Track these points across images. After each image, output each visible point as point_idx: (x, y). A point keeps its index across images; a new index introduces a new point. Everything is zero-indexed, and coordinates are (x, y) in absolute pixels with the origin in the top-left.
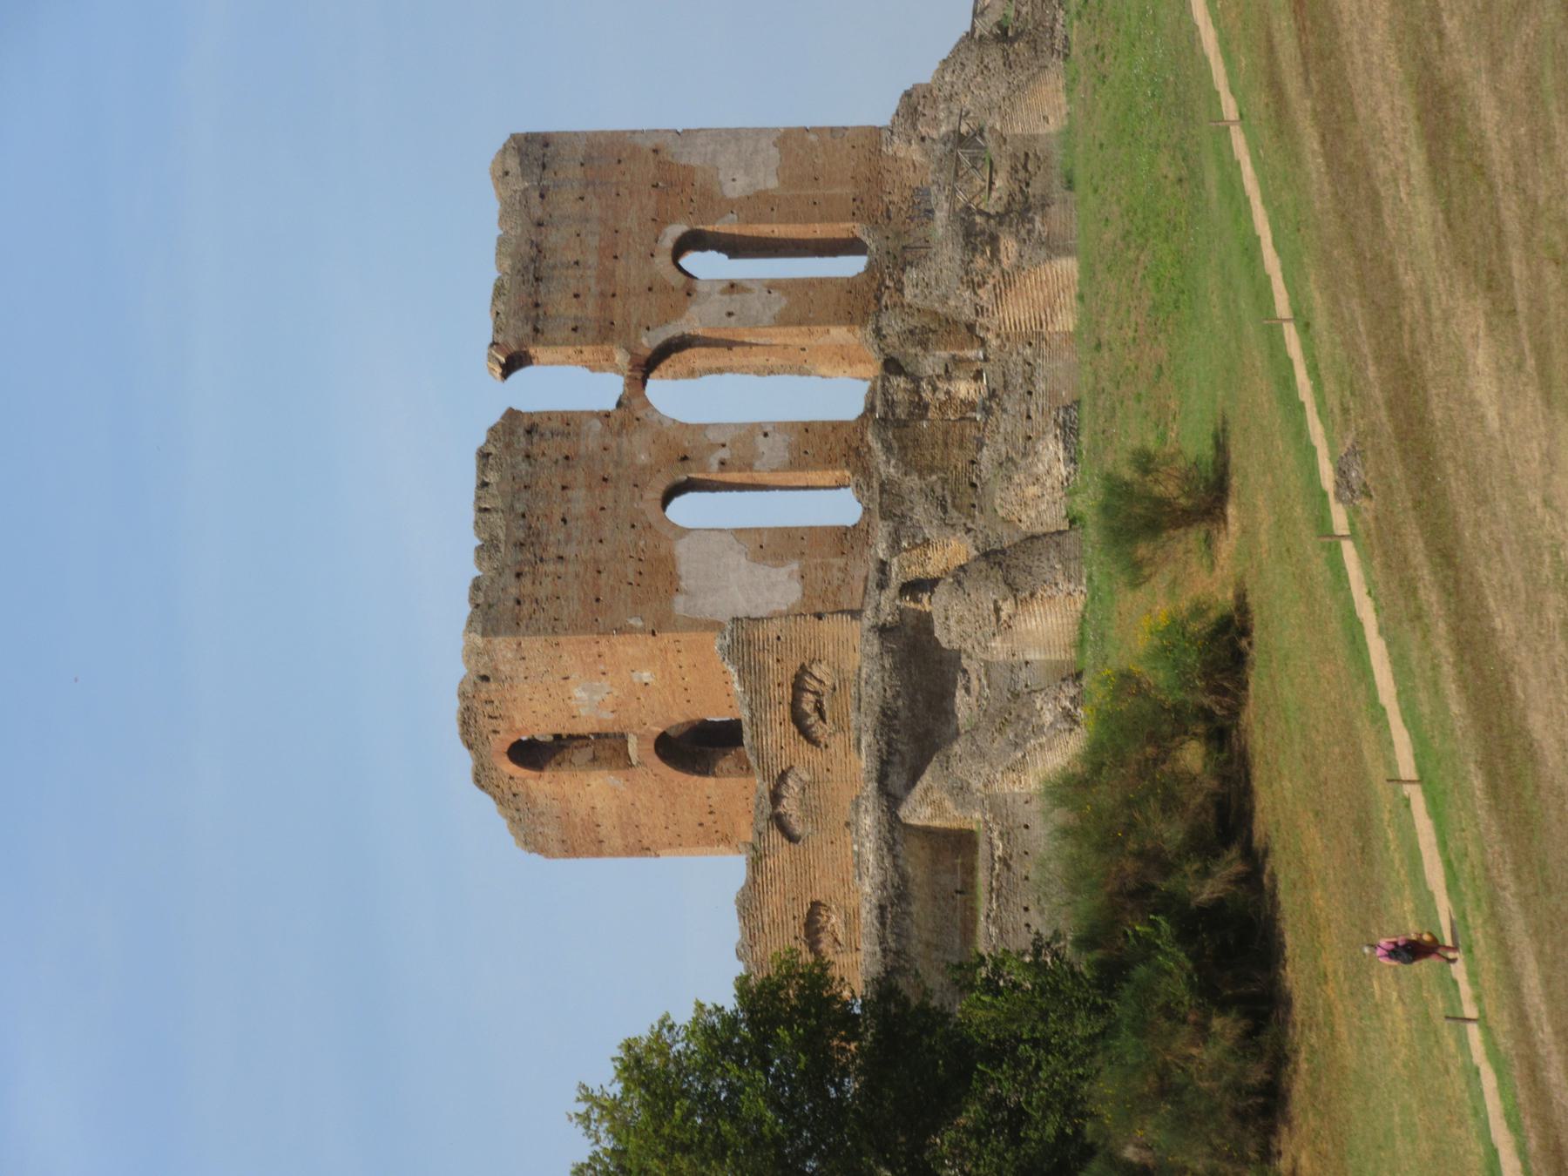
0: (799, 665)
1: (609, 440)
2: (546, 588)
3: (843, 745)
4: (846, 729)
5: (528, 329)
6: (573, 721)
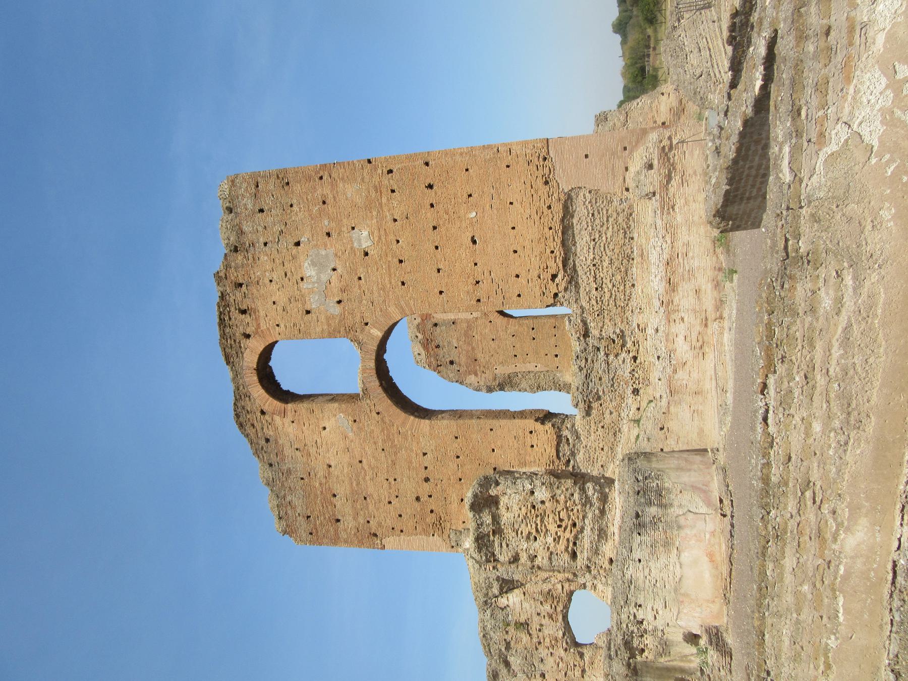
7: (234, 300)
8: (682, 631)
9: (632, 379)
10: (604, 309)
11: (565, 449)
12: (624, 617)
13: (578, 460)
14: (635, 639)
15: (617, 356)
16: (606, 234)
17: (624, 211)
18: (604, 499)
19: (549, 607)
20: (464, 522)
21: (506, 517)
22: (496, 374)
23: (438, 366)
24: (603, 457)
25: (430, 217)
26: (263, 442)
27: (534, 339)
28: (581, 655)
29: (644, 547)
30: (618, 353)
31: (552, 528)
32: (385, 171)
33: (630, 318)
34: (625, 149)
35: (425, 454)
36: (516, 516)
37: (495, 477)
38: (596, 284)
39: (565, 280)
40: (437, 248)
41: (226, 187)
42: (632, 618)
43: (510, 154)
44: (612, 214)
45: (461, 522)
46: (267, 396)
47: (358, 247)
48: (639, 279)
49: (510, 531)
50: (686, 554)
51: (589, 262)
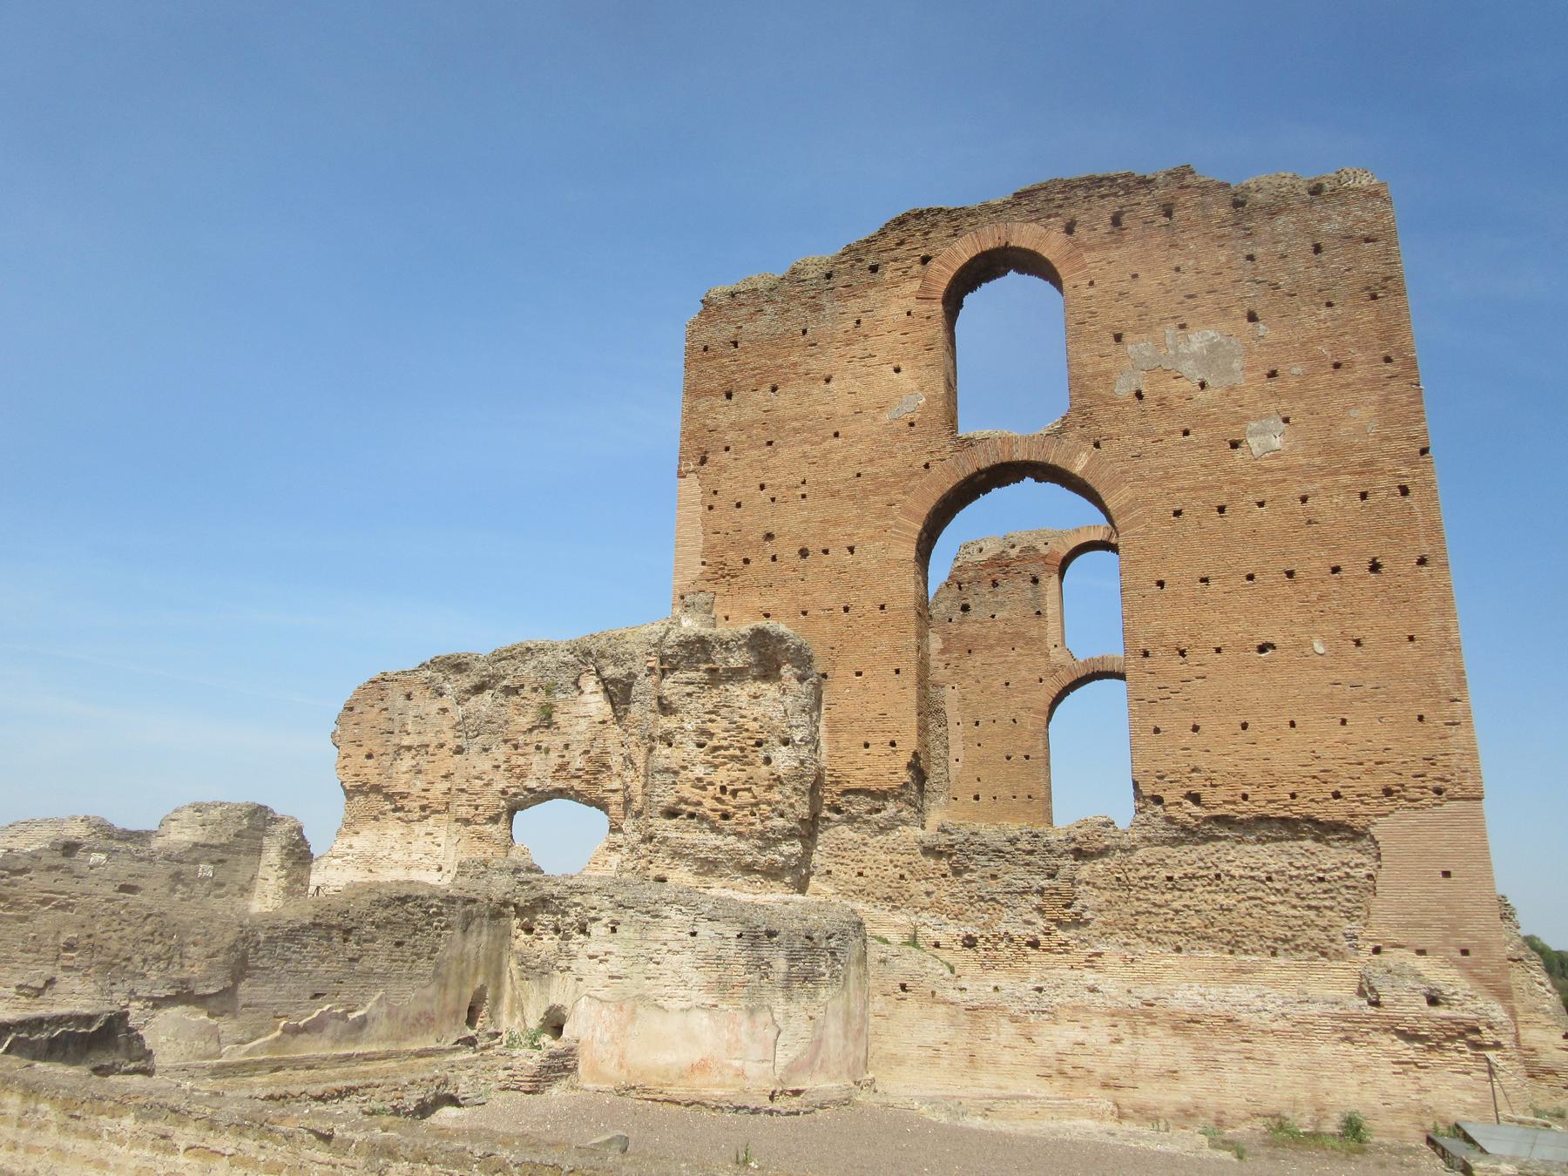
7: (1139, 204)
8: (568, 1004)
9: (994, 936)
10: (1130, 890)
11: (860, 806)
12: (594, 900)
13: (840, 828)
14: (551, 917)
15: (1040, 910)
16: (1281, 903)
17: (1332, 941)
18: (772, 873)
19: (578, 765)
20: (727, 618)
21: (740, 693)
22: (943, 687)
23: (959, 584)
24: (845, 874)
25: (1313, 563)
26: (870, 260)
27: (1008, 758)
28: (494, 820)
29: (718, 943)
30: (1044, 912)
31: (721, 777)
32: (1406, 482)
33: (1113, 939)
34: (1465, 952)
35: (851, 550)
36: (743, 712)
37: (812, 676)
38: (1180, 878)
39: (1189, 819)
40: (1250, 577)
41: (1364, 182)
42: (593, 914)
43: (1447, 724)
44: (1324, 916)
45: (727, 613)
46: (956, 268)
47: (1249, 429)
48: (1192, 962)
49: (715, 700)
50: (706, 1021)
51: (1226, 867)
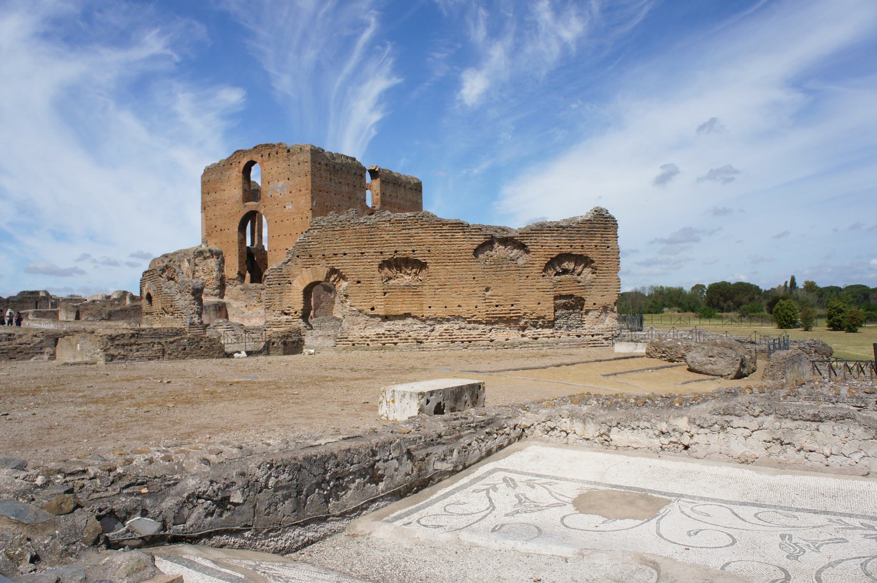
0: (594, 259)
1: (359, 200)
2: (324, 174)
3: (545, 287)
4: (555, 289)
5: (383, 179)
6: (267, 182)
11: (231, 282)
21: (209, 261)
